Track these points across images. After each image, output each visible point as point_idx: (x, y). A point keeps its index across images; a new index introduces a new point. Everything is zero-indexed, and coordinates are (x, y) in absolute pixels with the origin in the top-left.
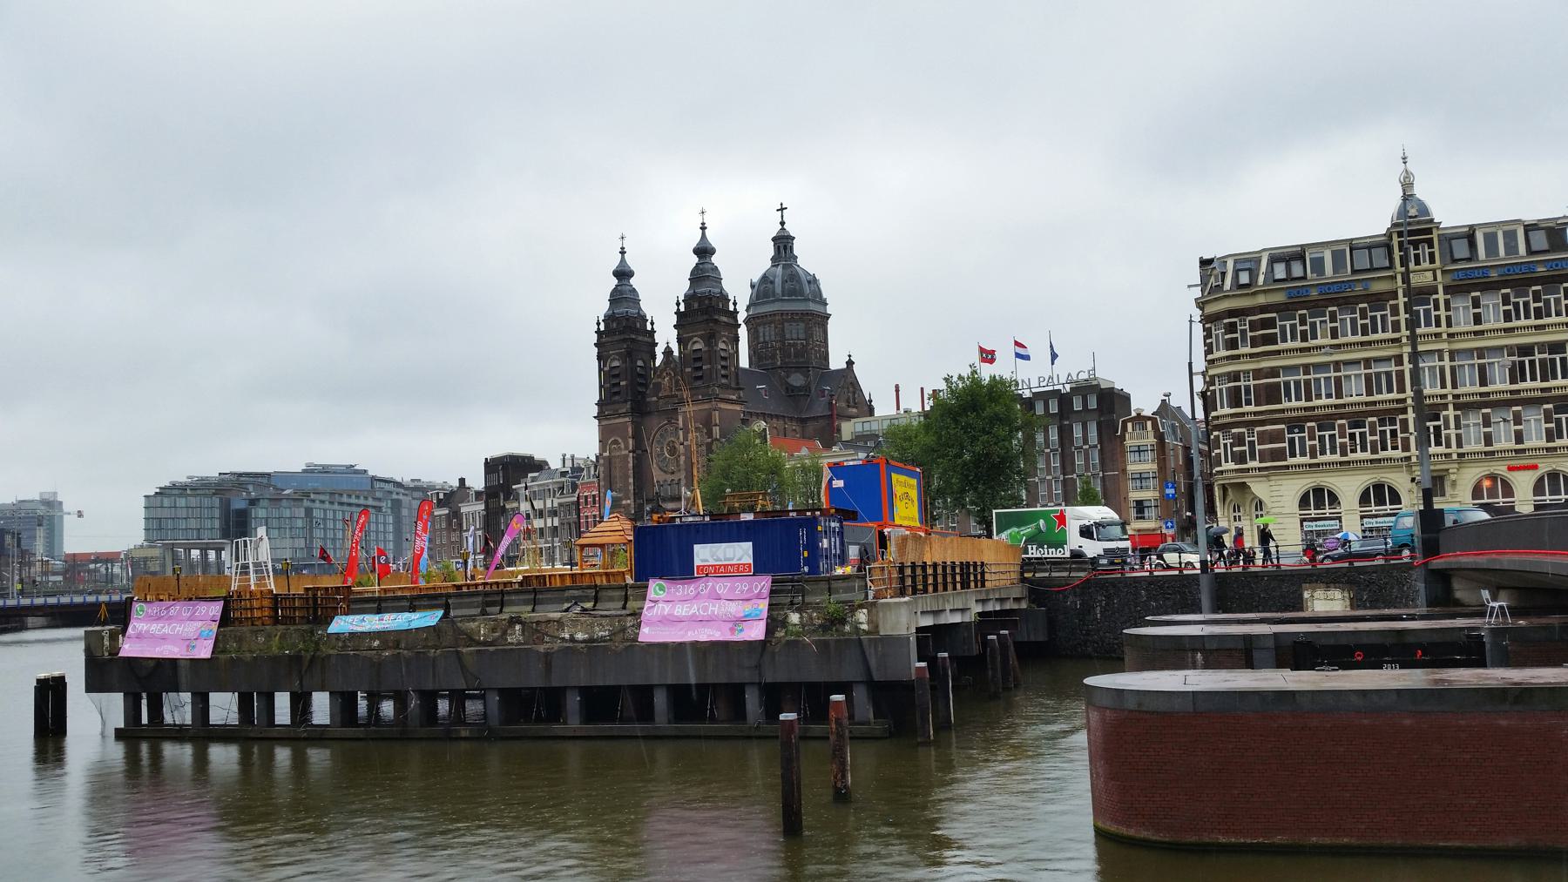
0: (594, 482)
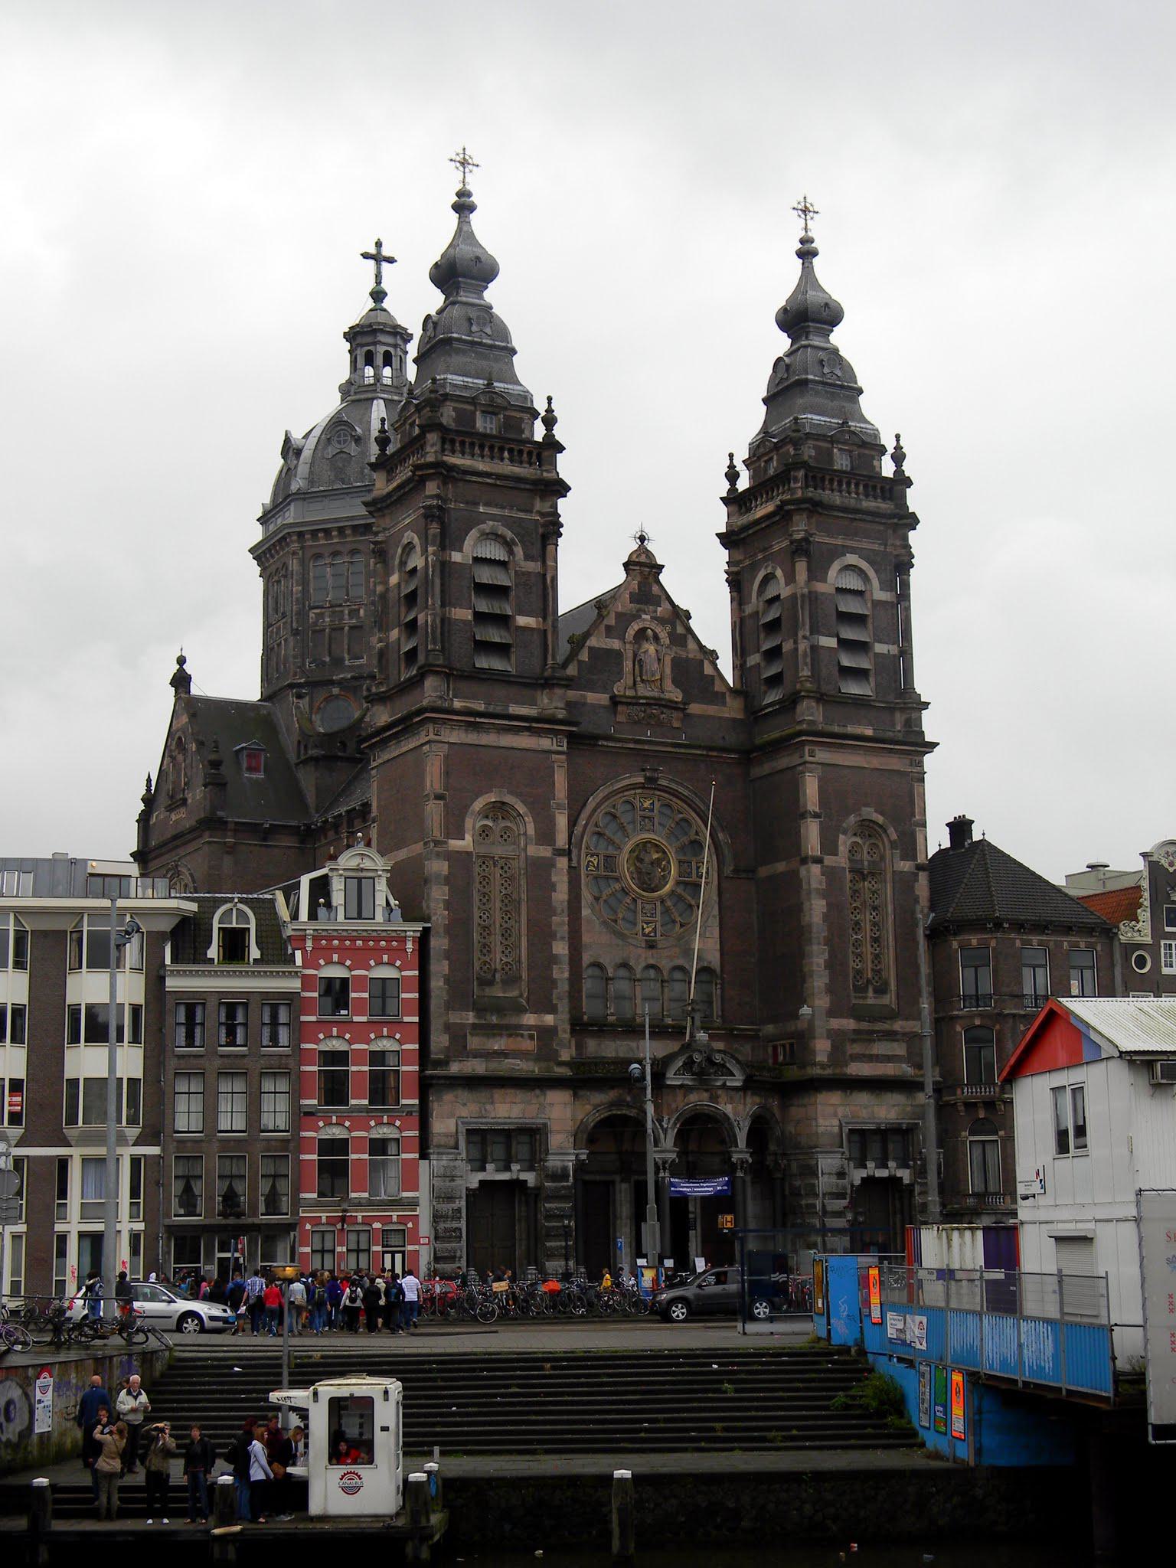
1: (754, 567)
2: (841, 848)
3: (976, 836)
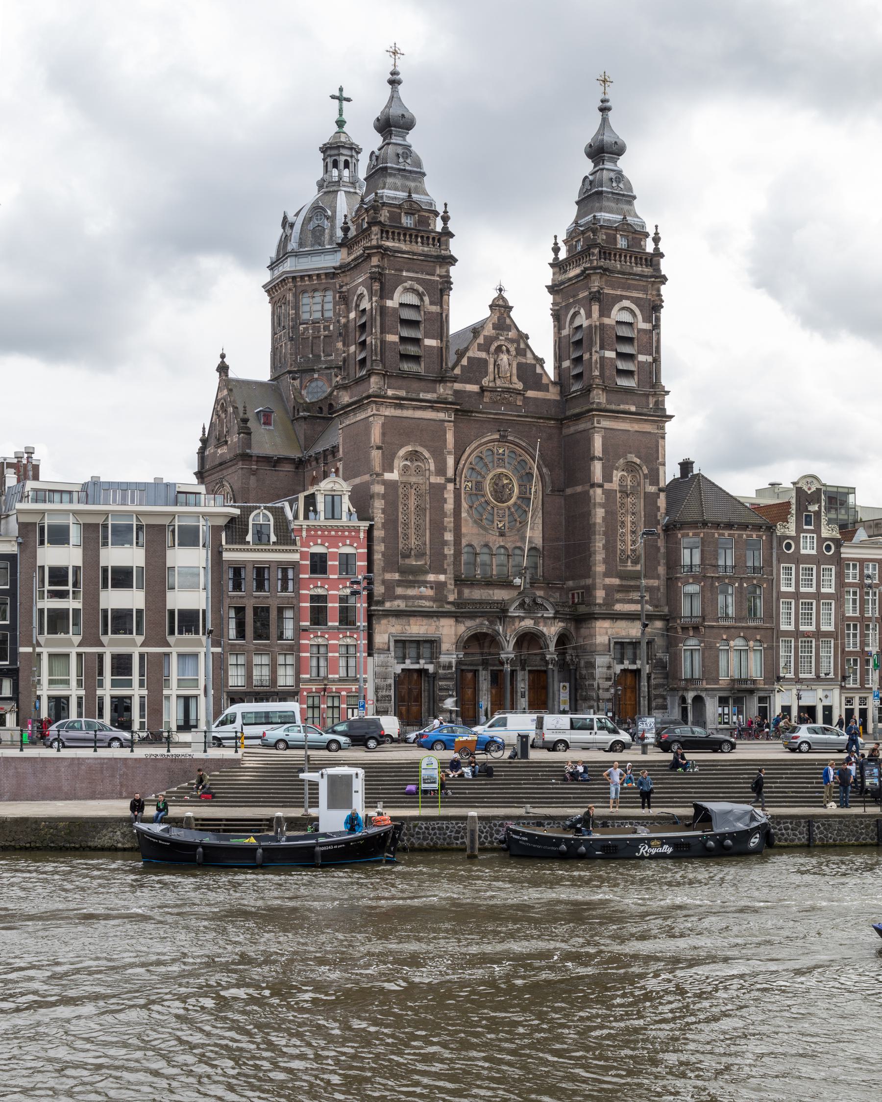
0: (357, 530)
1: (568, 307)
2: (614, 479)
3: (696, 472)
